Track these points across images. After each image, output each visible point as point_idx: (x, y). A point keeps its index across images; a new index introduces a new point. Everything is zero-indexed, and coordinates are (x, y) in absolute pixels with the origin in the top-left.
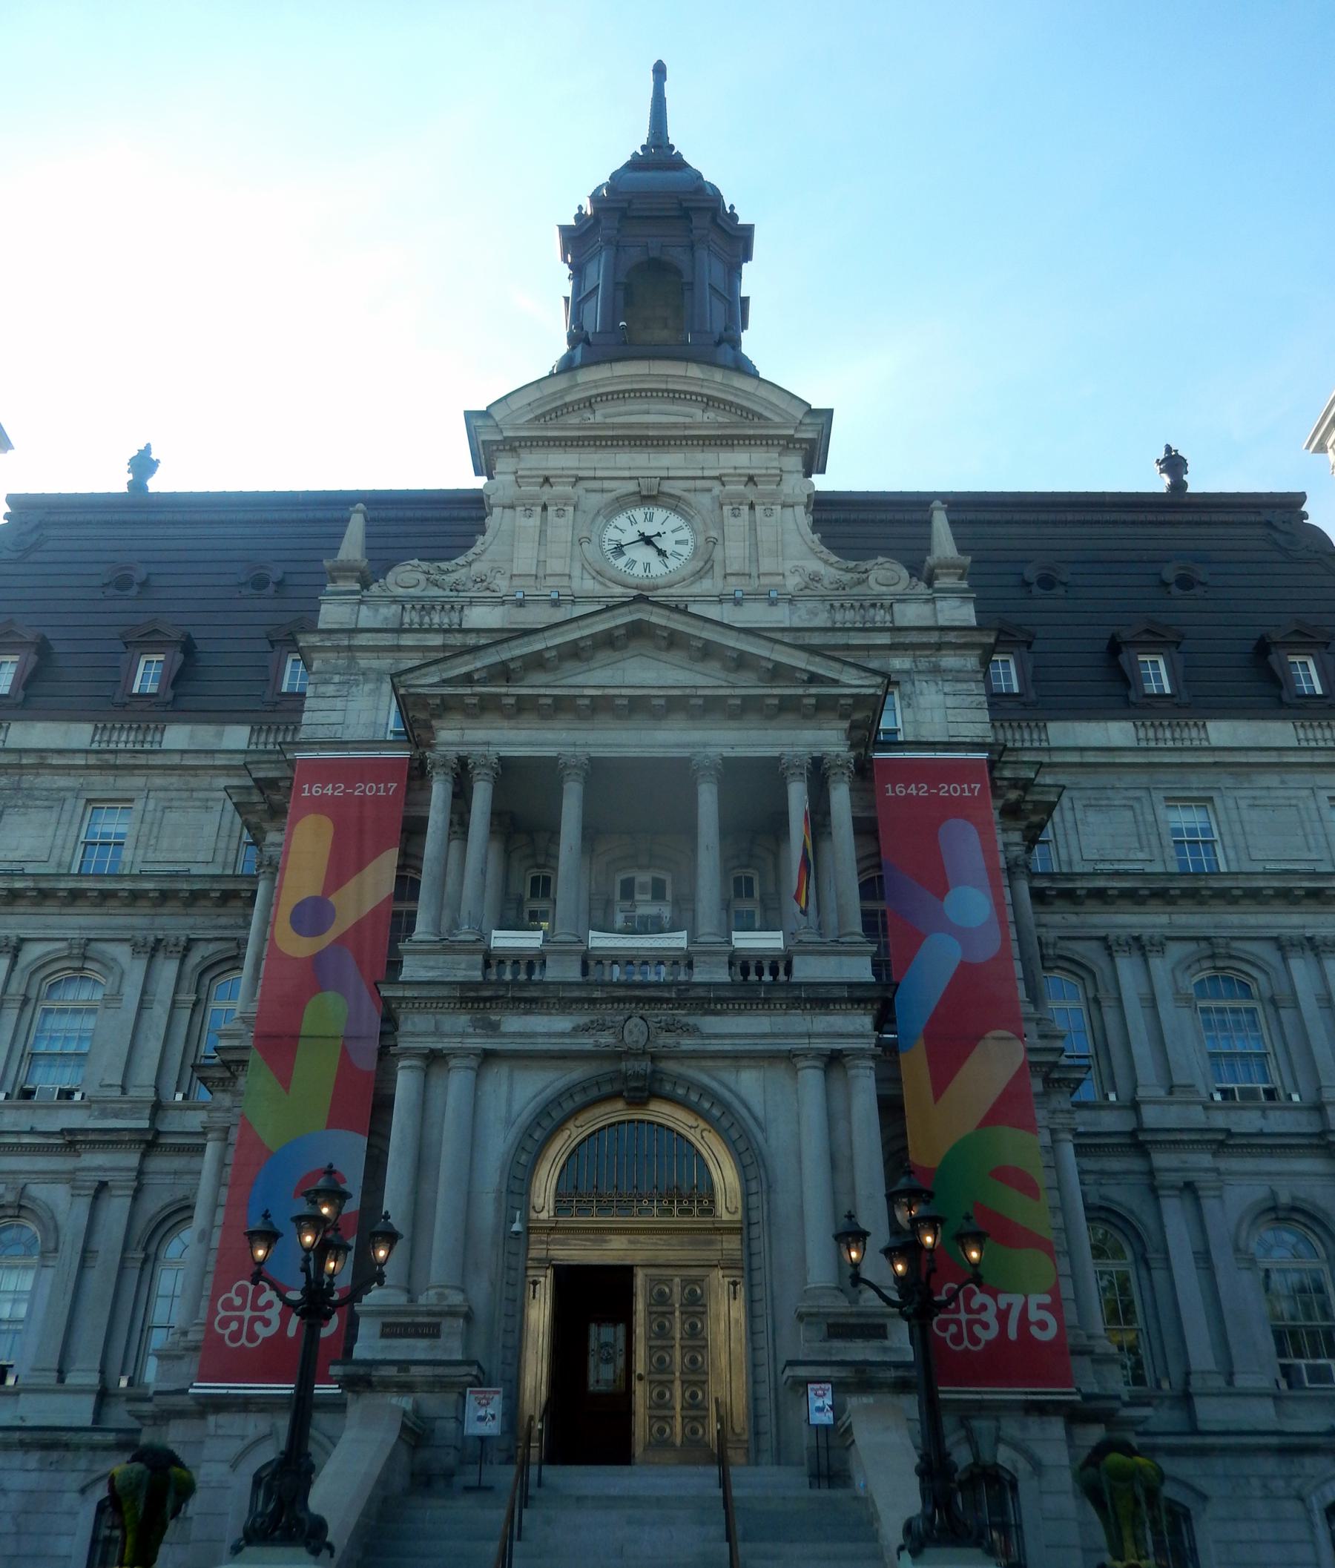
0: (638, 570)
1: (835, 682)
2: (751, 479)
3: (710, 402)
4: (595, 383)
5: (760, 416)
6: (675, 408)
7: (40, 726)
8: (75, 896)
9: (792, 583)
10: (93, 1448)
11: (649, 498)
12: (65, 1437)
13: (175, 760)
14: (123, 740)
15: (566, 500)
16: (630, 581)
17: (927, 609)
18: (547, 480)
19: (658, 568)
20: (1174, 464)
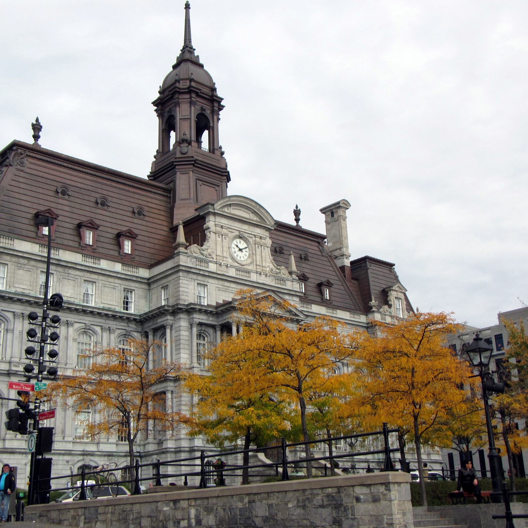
0: (239, 258)
1: (298, 316)
2: (261, 238)
3: (254, 212)
4: (233, 201)
5: (264, 220)
6: (246, 211)
7: (68, 252)
8: (92, 312)
9: (268, 269)
10: (118, 456)
11: (240, 237)
12: (115, 454)
13: (108, 273)
14: (90, 262)
15: (227, 235)
16: (240, 262)
17: (291, 283)
18: (222, 226)
19: (242, 259)
20: (297, 213)
